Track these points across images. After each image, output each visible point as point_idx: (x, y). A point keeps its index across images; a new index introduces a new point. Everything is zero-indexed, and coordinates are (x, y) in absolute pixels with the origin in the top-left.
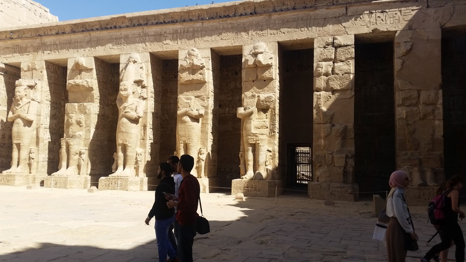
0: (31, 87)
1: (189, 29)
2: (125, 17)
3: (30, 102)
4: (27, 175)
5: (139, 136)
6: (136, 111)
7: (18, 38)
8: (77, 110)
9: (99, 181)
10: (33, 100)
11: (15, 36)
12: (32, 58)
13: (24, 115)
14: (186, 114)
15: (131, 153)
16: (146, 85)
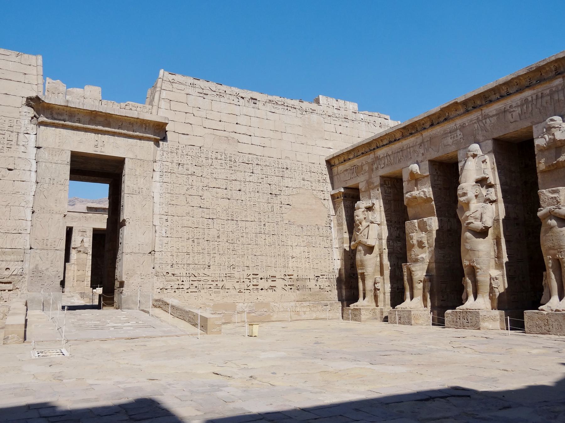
0: (369, 209)
1: (544, 92)
2: (456, 103)
3: (369, 226)
4: (374, 309)
5: (492, 253)
6: (481, 220)
7: (354, 157)
8: (417, 228)
9: (445, 315)
10: (372, 222)
11: (351, 157)
12: (367, 176)
13: (364, 240)
14: (551, 215)
15: (482, 277)
16: (493, 183)
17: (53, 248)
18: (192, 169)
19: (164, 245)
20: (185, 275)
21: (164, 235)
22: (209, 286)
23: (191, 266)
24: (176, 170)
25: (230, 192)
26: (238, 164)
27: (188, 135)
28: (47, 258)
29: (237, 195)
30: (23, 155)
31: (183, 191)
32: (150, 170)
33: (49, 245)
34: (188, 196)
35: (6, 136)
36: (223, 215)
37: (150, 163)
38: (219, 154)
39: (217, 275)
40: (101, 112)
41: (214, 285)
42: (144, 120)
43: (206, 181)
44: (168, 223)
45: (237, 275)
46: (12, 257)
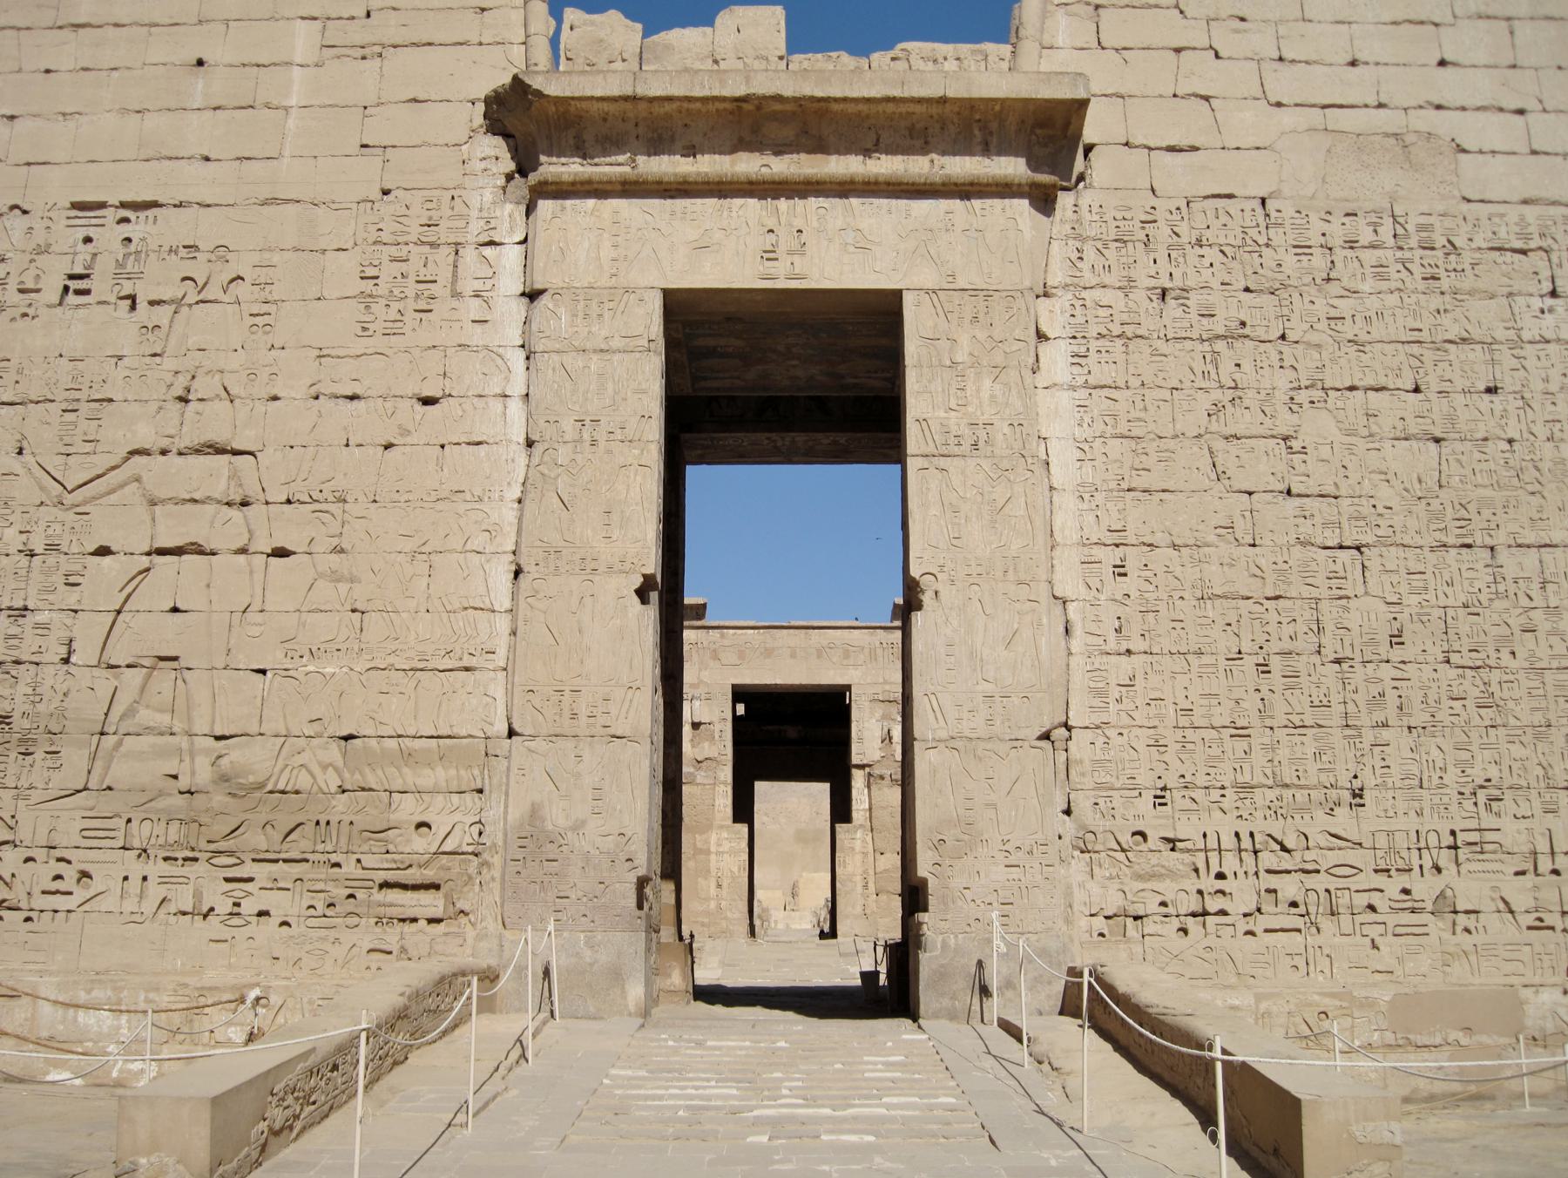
17: (600, 731)
18: (1228, 312)
19: (1115, 692)
20: (1228, 842)
21: (1112, 645)
22: (1362, 900)
23: (1262, 797)
24: (1148, 325)
25: (1439, 407)
26: (1468, 258)
27: (1195, 149)
28: (578, 776)
29: (1477, 414)
30: (476, 336)
31: (1195, 420)
32: (1018, 333)
33: (583, 712)
34: (1219, 445)
35: (414, 267)
36: (1412, 523)
37: (1020, 303)
38: (1361, 221)
39: (1401, 842)
40: (778, 98)
41: (1393, 886)
42: (970, 105)
43: (1307, 364)
44: (1130, 584)
45: (1512, 833)
46: (439, 775)
